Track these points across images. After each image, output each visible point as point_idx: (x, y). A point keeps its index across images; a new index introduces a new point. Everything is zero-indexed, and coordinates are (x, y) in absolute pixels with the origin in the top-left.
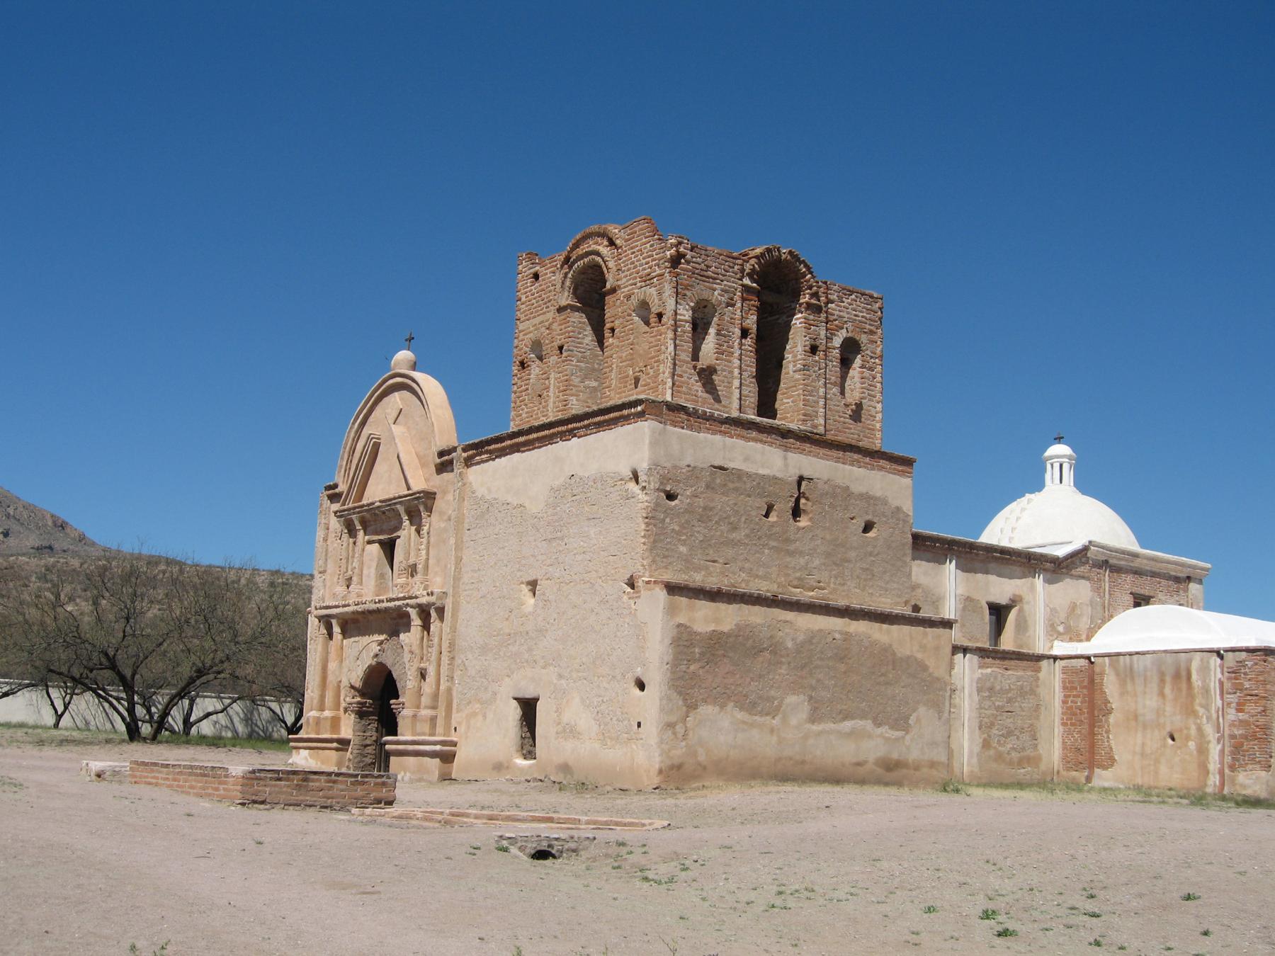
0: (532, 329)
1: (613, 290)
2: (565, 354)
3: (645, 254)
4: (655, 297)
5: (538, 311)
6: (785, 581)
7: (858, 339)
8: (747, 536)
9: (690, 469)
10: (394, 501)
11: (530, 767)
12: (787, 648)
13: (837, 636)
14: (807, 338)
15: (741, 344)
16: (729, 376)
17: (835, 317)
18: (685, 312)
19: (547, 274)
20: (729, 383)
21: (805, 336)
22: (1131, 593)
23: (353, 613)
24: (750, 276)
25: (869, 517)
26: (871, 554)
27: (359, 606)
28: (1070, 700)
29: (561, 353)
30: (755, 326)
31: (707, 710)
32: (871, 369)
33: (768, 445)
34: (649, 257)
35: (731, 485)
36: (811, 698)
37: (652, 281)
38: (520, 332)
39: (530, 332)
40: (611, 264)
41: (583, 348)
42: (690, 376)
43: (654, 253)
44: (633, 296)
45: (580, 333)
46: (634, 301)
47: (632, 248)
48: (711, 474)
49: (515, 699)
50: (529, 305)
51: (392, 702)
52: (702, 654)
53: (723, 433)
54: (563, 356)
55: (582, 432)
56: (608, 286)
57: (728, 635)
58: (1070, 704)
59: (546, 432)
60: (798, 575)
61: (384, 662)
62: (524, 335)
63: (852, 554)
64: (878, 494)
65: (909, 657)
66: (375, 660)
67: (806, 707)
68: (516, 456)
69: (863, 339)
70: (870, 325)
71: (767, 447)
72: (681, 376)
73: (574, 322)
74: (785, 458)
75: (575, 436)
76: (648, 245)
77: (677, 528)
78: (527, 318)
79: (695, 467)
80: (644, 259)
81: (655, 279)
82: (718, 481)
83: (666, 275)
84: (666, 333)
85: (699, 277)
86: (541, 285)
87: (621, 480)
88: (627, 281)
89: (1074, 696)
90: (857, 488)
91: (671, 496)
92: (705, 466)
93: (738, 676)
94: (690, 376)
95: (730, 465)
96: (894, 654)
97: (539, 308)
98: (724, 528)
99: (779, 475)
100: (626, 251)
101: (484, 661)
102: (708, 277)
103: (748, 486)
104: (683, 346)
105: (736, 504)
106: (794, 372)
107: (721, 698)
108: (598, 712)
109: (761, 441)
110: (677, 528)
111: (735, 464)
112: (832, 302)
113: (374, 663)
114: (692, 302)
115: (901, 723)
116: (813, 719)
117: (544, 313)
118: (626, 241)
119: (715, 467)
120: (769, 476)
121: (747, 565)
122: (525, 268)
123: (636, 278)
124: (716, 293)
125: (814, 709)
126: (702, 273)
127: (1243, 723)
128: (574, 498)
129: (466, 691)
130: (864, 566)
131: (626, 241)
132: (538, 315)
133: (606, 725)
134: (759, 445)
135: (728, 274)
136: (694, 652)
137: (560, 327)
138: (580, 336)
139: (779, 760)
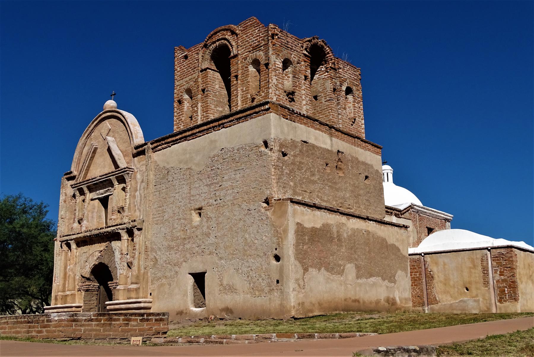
0: (184, 83)
1: (236, 56)
2: (206, 93)
3: (255, 36)
4: (263, 56)
5: (188, 74)
6: (336, 203)
7: (352, 88)
8: (319, 179)
9: (292, 141)
10: (108, 175)
11: (202, 311)
14: (332, 85)
16: (301, 99)
17: (342, 76)
18: (279, 63)
19: (193, 55)
20: (301, 102)
21: (331, 84)
23: (84, 237)
24: (306, 49)
27: (88, 233)
28: (413, 274)
29: (204, 93)
31: (313, 271)
32: (358, 103)
33: (324, 133)
34: (257, 36)
36: (356, 265)
37: (260, 48)
38: (177, 86)
39: (183, 85)
40: (234, 43)
41: (215, 90)
42: (284, 97)
43: (261, 34)
44: (248, 58)
45: (213, 83)
46: (249, 60)
47: (246, 34)
49: (189, 274)
50: (182, 72)
51: (109, 283)
53: (305, 124)
54: (205, 94)
55: (228, 124)
56: (232, 54)
57: (320, 229)
58: (413, 276)
59: (205, 127)
60: (341, 201)
61: (103, 262)
62: (180, 87)
63: (362, 192)
64: (369, 163)
66: (98, 261)
68: (184, 144)
69: (354, 88)
70: (356, 82)
73: (210, 77)
74: (331, 140)
75: (224, 127)
76: (257, 31)
77: (288, 172)
78: (181, 78)
79: (294, 141)
80: (254, 38)
81: (262, 48)
82: (305, 149)
83: (269, 43)
84: (272, 73)
85: (284, 47)
86: (189, 61)
87: (256, 147)
88: (244, 51)
89: (415, 272)
90: (361, 159)
91: (284, 155)
92: (299, 140)
93: (325, 252)
94: (284, 97)
97: (189, 73)
98: (308, 174)
100: (242, 36)
101: (168, 255)
102: (288, 47)
104: (279, 80)
105: (313, 162)
106: (325, 102)
108: (248, 276)
110: (288, 172)
111: (312, 141)
113: (97, 263)
114: (282, 59)
117: (192, 74)
118: (242, 31)
119: (303, 141)
122: (179, 55)
123: (249, 48)
124: (292, 56)
126: (286, 45)
127: (504, 281)
128: (224, 161)
129: (156, 273)
131: (242, 31)
132: (188, 76)
133: (254, 283)
135: (297, 47)
136: (305, 239)
137: (203, 80)
138: (214, 84)
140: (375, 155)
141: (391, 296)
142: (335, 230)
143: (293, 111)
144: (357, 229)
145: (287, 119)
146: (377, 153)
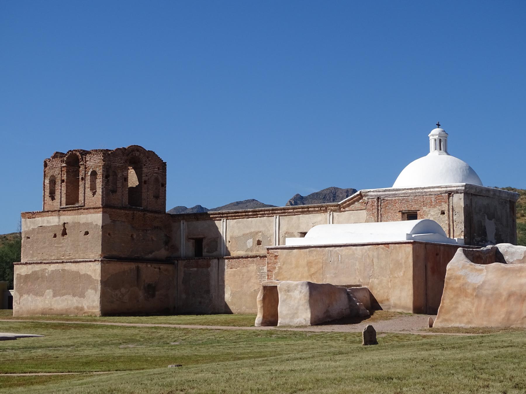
8: (48, 244)
12: (46, 277)
13: (61, 270)
15: (61, 186)
18: (47, 181)
22: (399, 211)
25: (86, 230)
26: (87, 242)
30: (66, 178)
31: (25, 296)
35: (44, 231)
36: (53, 290)
48: (39, 229)
52: (23, 281)
57: (30, 275)
63: (80, 244)
65: (84, 275)
67: (51, 294)
71: (54, 217)
72: (47, 200)
74: (59, 218)
82: (40, 231)
90: (82, 222)
95: (44, 225)
96: (80, 273)
99: (57, 224)
103: (48, 230)
107: (28, 293)
109: (52, 216)
112: (88, 161)
115: (82, 295)
116: (54, 296)
120: (54, 225)
121: (48, 253)
125: (54, 293)
130: (84, 246)
134: (52, 217)
139: (44, 309)
140: (96, 215)
141: (80, 306)
142: (40, 273)
143: (33, 212)
144: (55, 270)
145: (30, 218)
146: (98, 212)
